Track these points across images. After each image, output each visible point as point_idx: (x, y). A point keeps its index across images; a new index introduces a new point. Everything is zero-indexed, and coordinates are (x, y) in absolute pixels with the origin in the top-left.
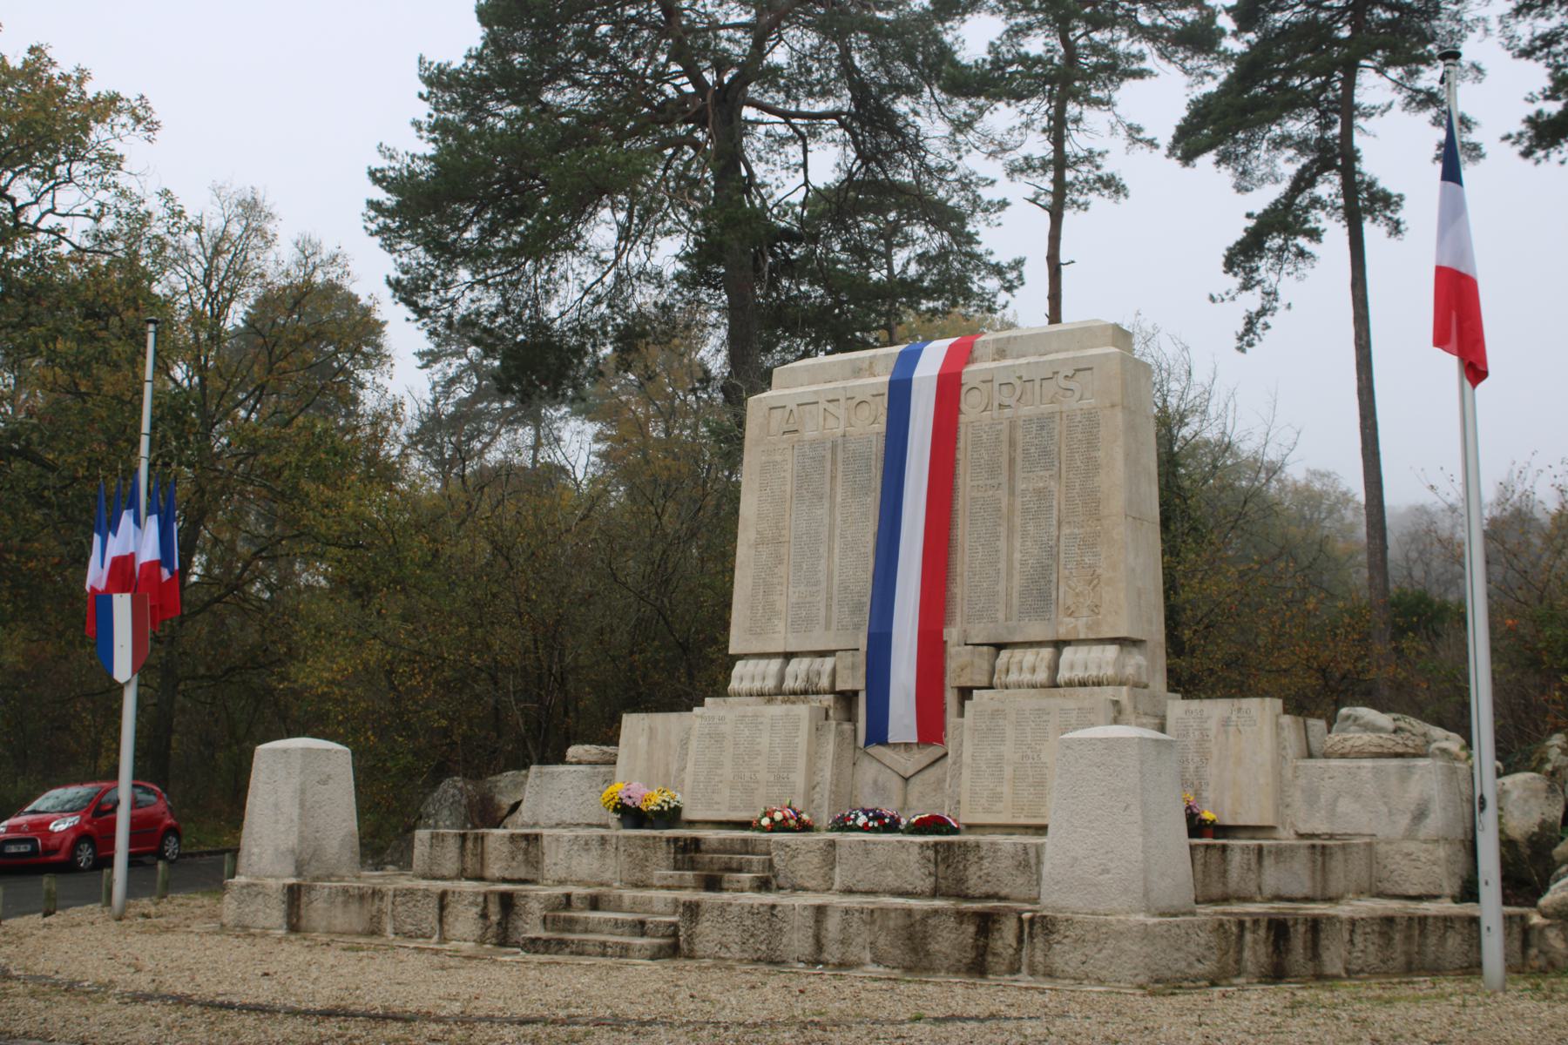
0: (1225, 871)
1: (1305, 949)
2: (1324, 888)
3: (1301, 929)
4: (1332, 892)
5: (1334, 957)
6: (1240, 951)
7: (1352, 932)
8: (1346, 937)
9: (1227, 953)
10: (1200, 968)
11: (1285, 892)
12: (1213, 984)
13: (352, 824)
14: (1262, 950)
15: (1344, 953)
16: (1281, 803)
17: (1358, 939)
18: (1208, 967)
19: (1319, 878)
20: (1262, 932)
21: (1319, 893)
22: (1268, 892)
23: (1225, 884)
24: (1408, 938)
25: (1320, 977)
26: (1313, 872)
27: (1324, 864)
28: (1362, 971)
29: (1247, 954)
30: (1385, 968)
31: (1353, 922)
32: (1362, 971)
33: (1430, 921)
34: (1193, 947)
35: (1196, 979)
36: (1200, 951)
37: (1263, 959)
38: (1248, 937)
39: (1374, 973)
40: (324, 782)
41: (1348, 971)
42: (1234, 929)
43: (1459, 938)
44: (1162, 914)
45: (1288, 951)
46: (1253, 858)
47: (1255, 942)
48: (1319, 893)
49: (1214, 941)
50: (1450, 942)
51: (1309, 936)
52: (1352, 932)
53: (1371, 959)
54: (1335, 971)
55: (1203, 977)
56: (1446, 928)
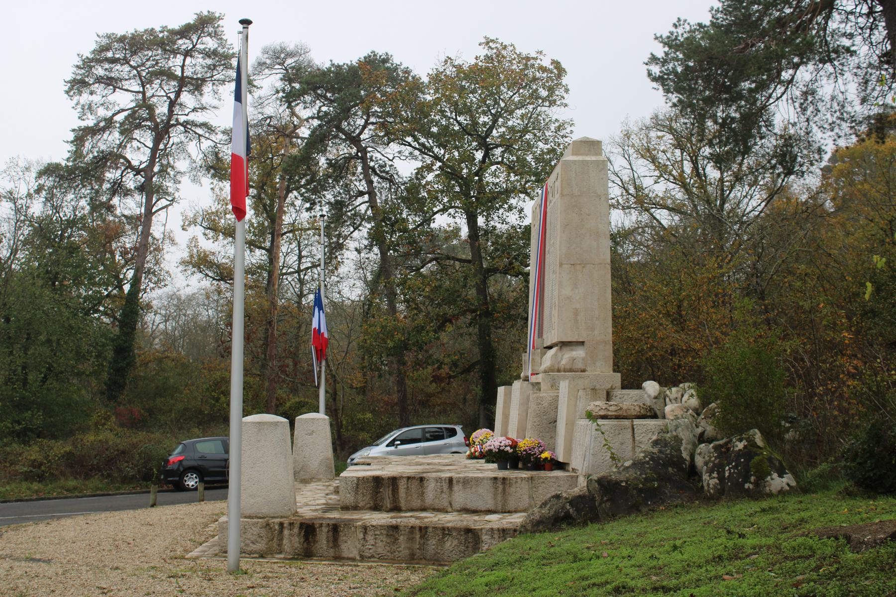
0: (423, 493)
1: (328, 541)
2: (503, 505)
3: (325, 529)
4: (511, 505)
5: (350, 546)
6: (282, 539)
7: (365, 533)
8: (361, 536)
9: (272, 540)
10: (253, 547)
11: (470, 506)
12: (262, 556)
13: (330, 453)
14: (296, 540)
15: (359, 546)
16: (569, 450)
17: (370, 538)
18: (260, 546)
19: (499, 497)
20: (296, 530)
21: (500, 508)
22: (457, 505)
23: (423, 501)
24: (411, 539)
25: (338, 558)
26: (495, 495)
27: (504, 490)
28: (372, 556)
29: (285, 542)
30: (391, 556)
31: (365, 529)
32: (372, 556)
33: (430, 530)
34: (249, 536)
35: (251, 553)
36: (253, 538)
37: (297, 545)
38: (286, 532)
39: (381, 558)
40: (311, 434)
41: (362, 557)
42: (277, 527)
43: (456, 542)
44: (245, 517)
45: (315, 542)
46: (445, 486)
47: (290, 535)
48: (500, 508)
49: (263, 532)
50: (448, 544)
51: (331, 534)
52: (365, 533)
53: (380, 550)
54: (351, 556)
55: (255, 552)
56: (444, 535)
